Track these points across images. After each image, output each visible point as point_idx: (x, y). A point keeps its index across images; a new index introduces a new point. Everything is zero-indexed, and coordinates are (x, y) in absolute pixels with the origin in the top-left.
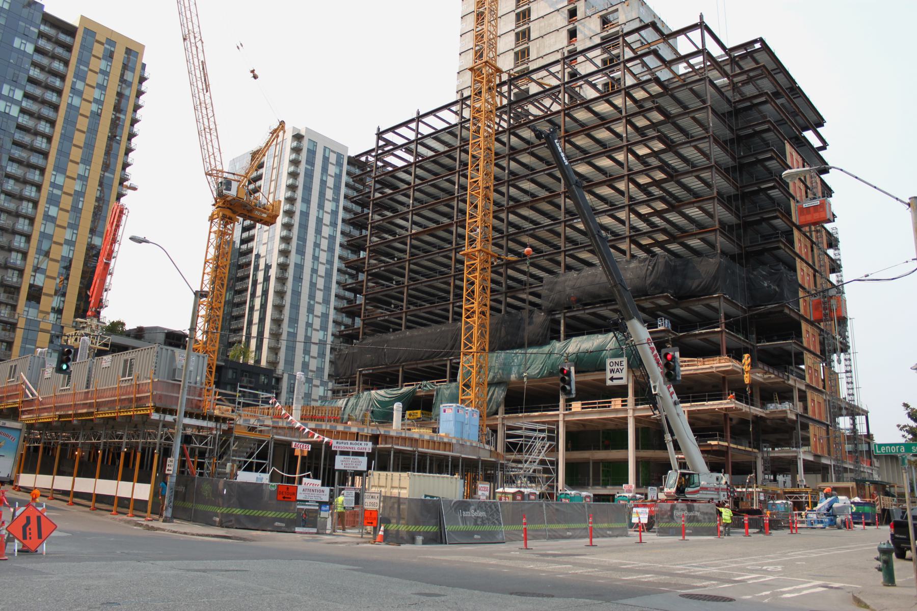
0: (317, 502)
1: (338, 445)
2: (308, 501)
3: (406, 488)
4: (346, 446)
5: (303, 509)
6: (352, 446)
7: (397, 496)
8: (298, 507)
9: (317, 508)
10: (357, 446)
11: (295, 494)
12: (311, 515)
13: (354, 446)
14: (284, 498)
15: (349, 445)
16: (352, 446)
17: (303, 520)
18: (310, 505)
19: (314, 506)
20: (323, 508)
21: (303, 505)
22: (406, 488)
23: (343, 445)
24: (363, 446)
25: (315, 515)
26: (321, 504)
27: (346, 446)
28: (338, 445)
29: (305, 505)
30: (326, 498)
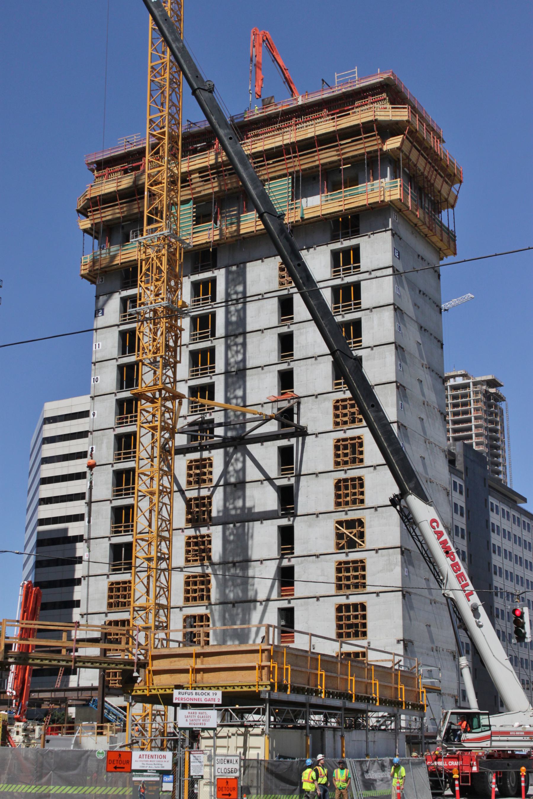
0: (158, 771)
1: (181, 696)
2: (146, 771)
3: (259, 748)
4: (190, 697)
5: (140, 781)
6: (197, 697)
7: (256, 758)
8: (134, 779)
9: (158, 779)
10: (203, 697)
11: (129, 762)
12: (150, 788)
13: (200, 697)
14: (115, 768)
15: (194, 696)
16: (197, 697)
17: (141, 796)
18: (149, 776)
19: (154, 776)
20: (166, 778)
21: (139, 776)
22: (259, 748)
23: (186, 696)
24: (211, 696)
25: (155, 788)
26: (163, 773)
27: (190, 697)
28: (181, 696)
29: (143, 776)
30: (168, 766)
